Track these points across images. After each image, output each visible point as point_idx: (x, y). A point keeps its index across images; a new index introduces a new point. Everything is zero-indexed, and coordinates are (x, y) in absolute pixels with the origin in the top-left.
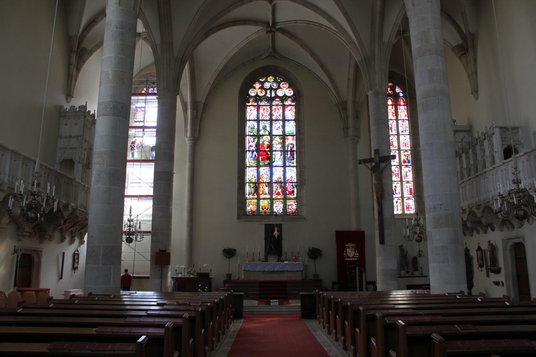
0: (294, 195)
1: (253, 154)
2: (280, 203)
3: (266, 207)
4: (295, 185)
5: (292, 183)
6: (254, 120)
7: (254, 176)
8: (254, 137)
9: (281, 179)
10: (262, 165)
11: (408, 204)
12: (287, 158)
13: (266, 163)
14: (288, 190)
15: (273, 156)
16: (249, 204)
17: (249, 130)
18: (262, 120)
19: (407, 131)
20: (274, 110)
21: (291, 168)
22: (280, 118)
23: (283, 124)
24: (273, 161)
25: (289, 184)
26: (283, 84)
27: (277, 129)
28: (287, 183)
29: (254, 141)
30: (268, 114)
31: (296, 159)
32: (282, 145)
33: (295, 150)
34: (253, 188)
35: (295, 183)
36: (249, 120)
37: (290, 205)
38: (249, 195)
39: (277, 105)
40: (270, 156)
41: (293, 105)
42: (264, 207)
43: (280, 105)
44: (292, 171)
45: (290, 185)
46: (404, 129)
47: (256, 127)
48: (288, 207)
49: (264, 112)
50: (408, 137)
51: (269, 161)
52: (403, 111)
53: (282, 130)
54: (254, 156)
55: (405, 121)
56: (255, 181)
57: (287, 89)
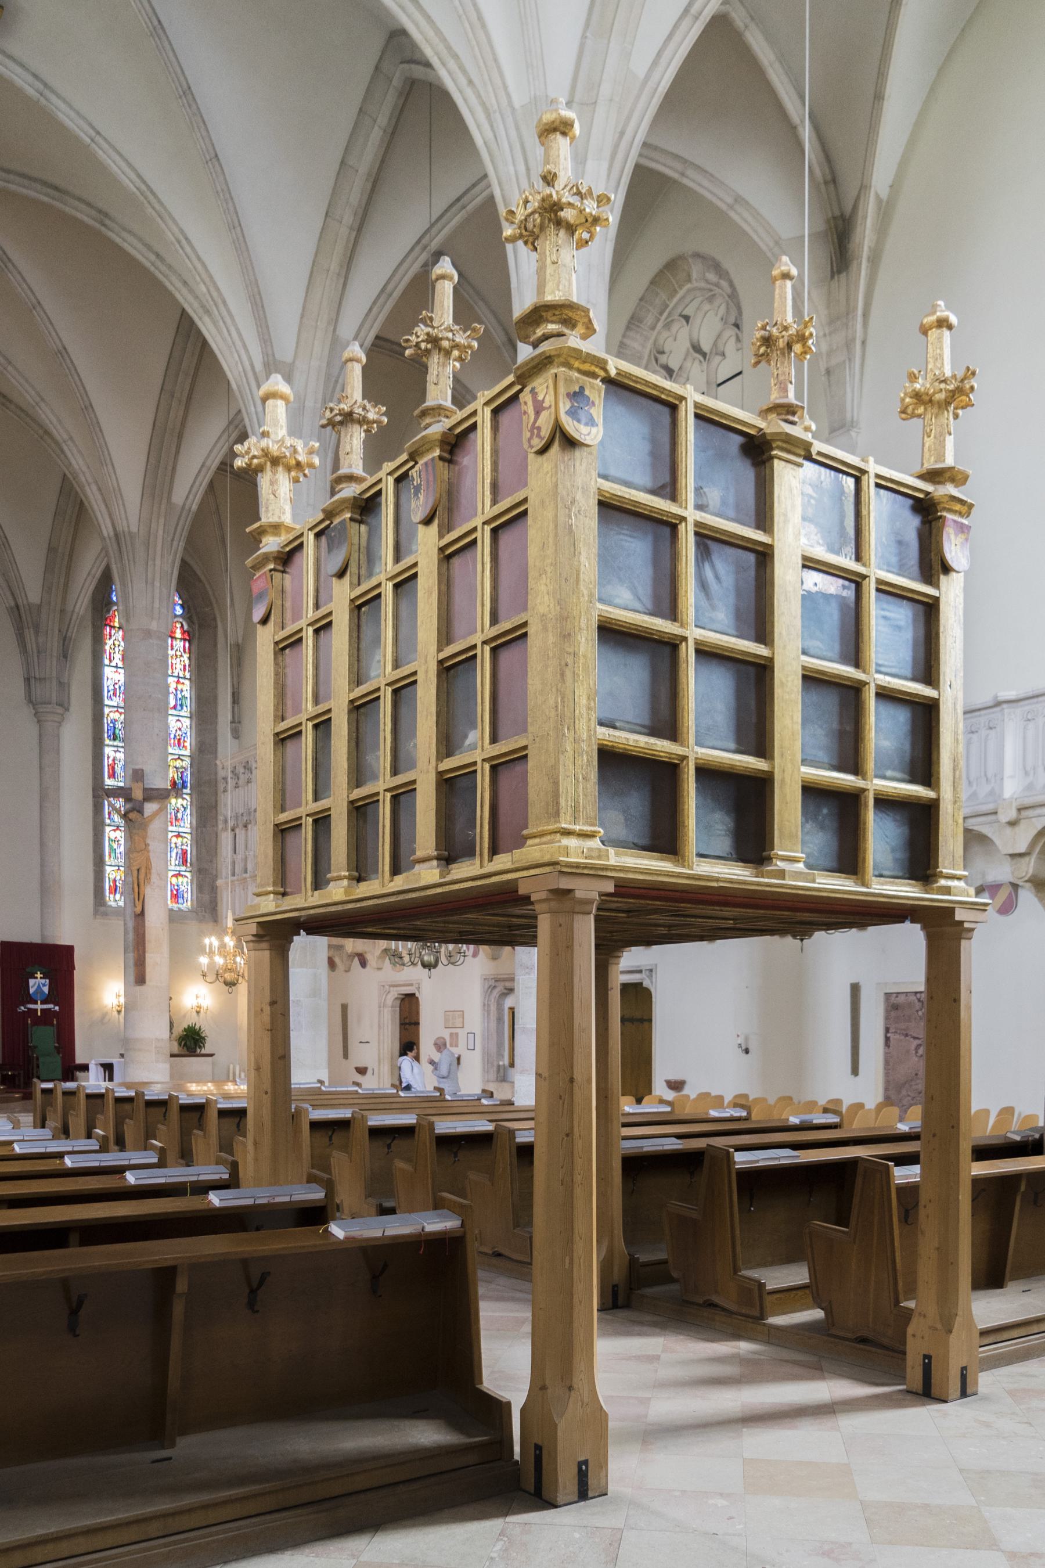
11: (176, 887)
19: (185, 708)
46: (179, 703)
50: (187, 722)
52: (178, 653)
55: (181, 680)
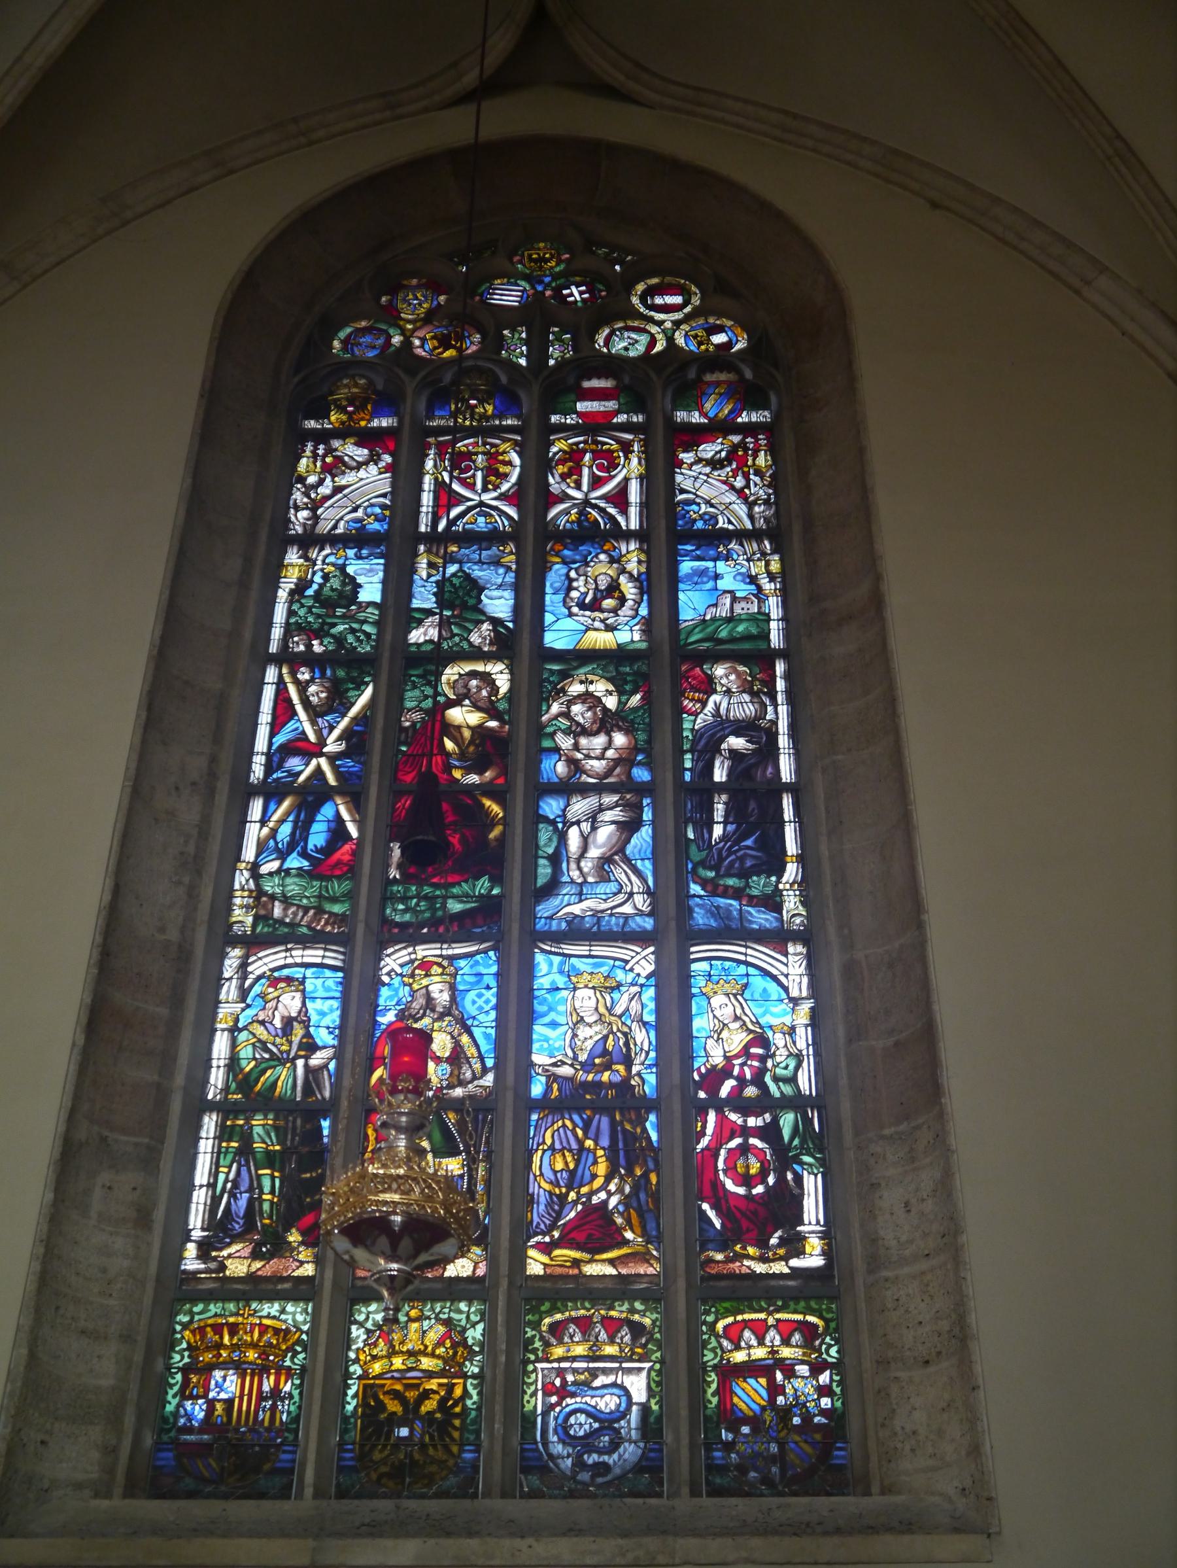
0: (794, 1245)
1: (310, 821)
2: (610, 1350)
3: (426, 1395)
4: (803, 1130)
5: (764, 1104)
6: (359, 539)
7: (298, 1032)
8: (341, 673)
9: (628, 1062)
10: (403, 926)
12: (696, 854)
13: (455, 907)
14: (718, 1186)
15: (545, 834)
16: (208, 1357)
17: (291, 613)
18: (434, 539)
20: (562, 462)
21: (760, 954)
22: (621, 520)
23: (649, 562)
24: (540, 882)
25: (722, 1120)
26: (651, 291)
27: (595, 606)
28: (702, 1110)
29: (337, 701)
30: (495, 494)
31: (801, 859)
32: (642, 736)
33: (786, 769)
34: (270, 1160)
35: (797, 1103)
36: (309, 540)
37: (751, 1369)
38: (205, 1250)
39: (594, 426)
40: (502, 839)
41: (750, 430)
42: (396, 1395)
43: (627, 427)
44: (759, 983)
45: (745, 1131)
47: (371, 591)
48: (724, 1391)
49: (463, 482)
51: (496, 880)
53: (644, 611)
54: (318, 837)
56: (308, 1090)
57: (687, 319)
